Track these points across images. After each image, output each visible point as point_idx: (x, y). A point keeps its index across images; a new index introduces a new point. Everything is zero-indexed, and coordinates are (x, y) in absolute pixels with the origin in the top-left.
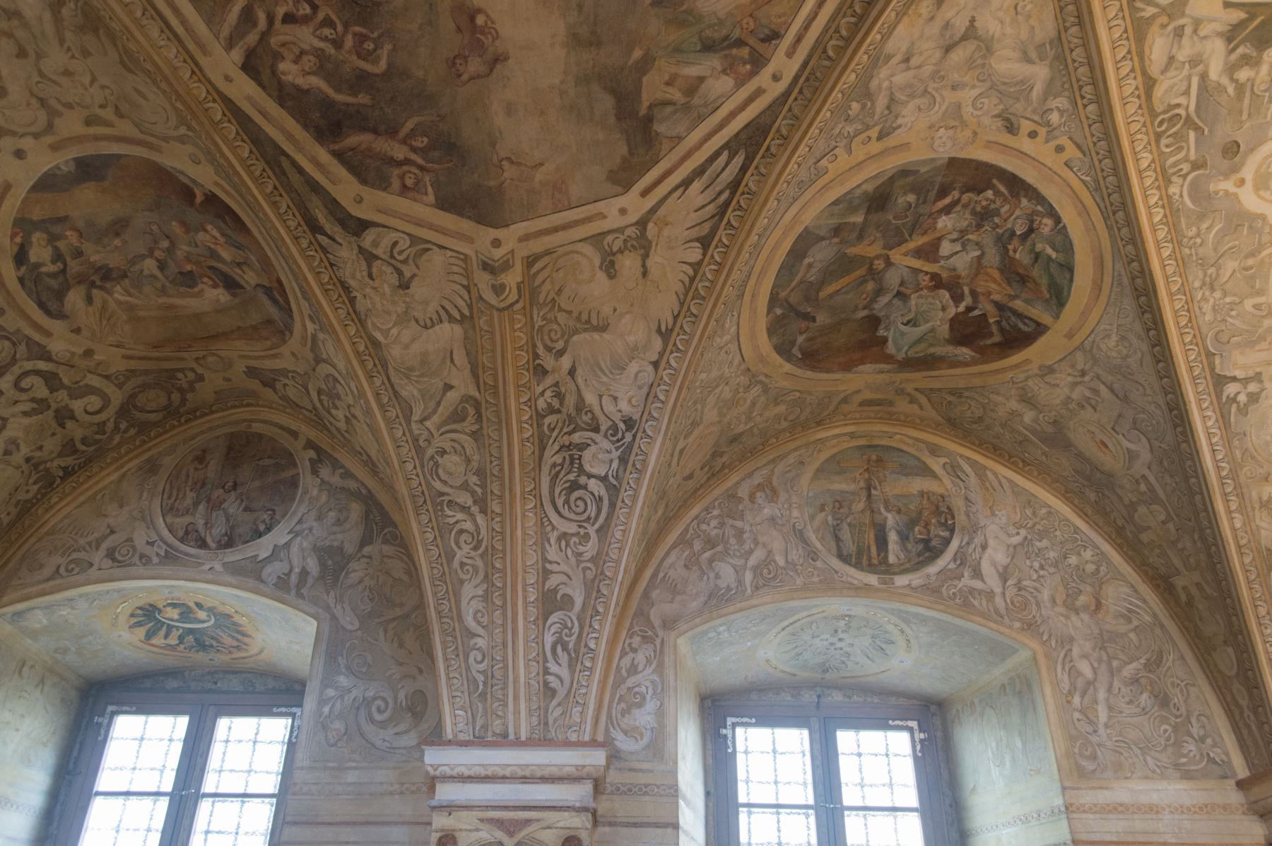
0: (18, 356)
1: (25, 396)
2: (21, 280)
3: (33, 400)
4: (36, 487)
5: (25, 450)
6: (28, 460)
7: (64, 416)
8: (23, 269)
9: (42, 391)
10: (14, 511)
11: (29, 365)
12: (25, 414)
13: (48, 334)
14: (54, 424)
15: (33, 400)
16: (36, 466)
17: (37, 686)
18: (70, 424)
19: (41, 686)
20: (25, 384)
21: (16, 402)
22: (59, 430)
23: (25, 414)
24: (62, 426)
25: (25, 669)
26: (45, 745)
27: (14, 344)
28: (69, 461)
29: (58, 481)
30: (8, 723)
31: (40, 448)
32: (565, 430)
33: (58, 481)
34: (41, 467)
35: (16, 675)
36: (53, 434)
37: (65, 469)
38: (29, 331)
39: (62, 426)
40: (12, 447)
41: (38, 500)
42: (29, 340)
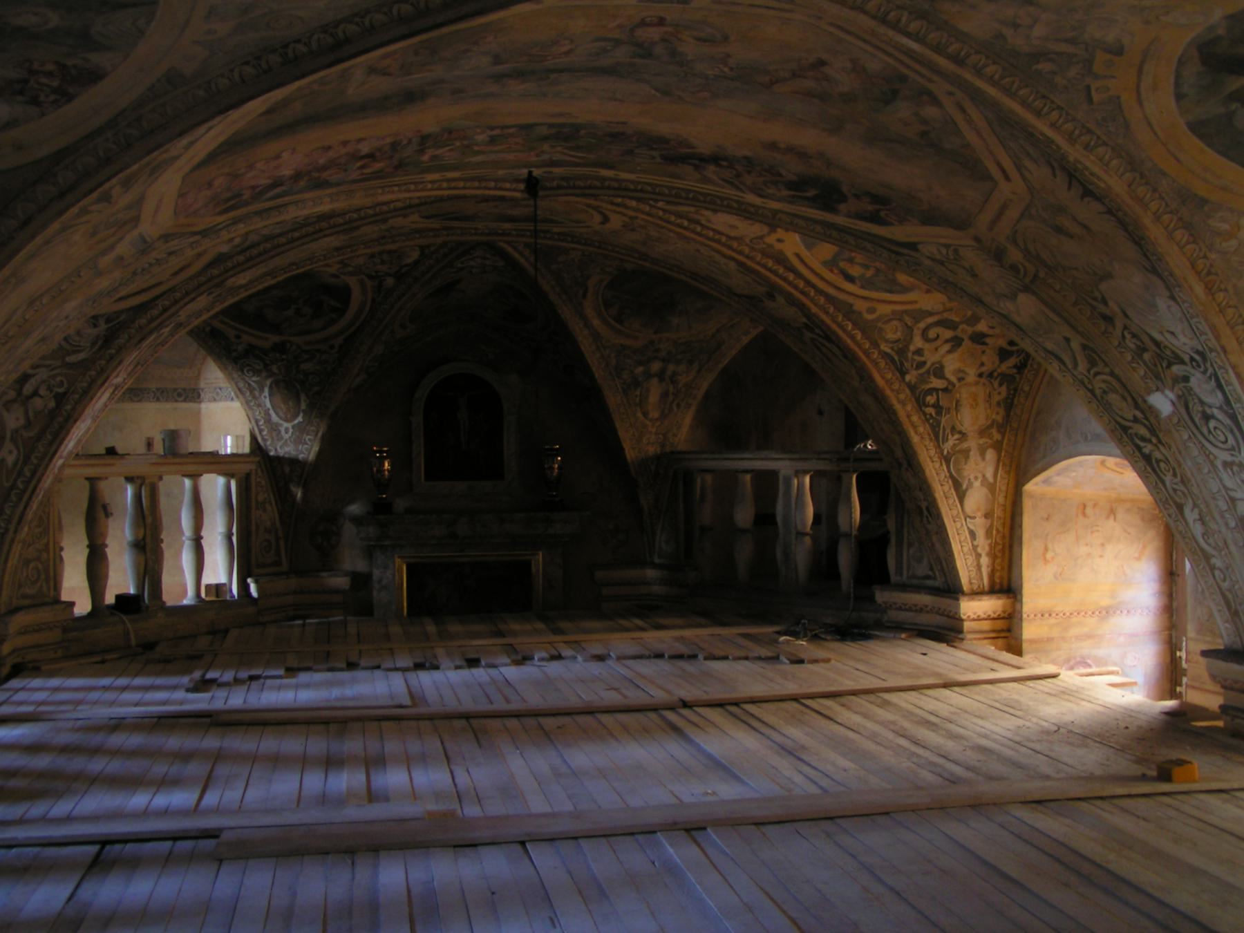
0: (909, 324)
1: (939, 342)
2: (862, 287)
3: (947, 341)
4: (1004, 388)
5: (972, 375)
6: (980, 375)
7: (979, 338)
8: (857, 281)
9: (948, 334)
10: (1002, 411)
11: (922, 325)
12: (949, 352)
13: (916, 302)
14: (979, 347)
15: (947, 341)
16: (991, 375)
17: (1108, 517)
18: (988, 340)
19: (1112, 517)
20: (932, 334)
21: (936, 349)
22: (984, 347)
23: (949, 352)
24: (985, 344)
25: (1089, 511)
26: (1138, 559)
27: (900, 320)
28: (1012, 361)
29: (1017, 376)
30: (1089, 555)
31: (982, 364)
32: (1164, 365)
33: (1017, 376)
34: (995, 374)
35: (1081, 517)
36: (983, 352)
37: (1015, 366)
38: (898, 308)
39: (985, 344)
40: (961, 375)
41: (1014, 395)
42: (906, 312)
